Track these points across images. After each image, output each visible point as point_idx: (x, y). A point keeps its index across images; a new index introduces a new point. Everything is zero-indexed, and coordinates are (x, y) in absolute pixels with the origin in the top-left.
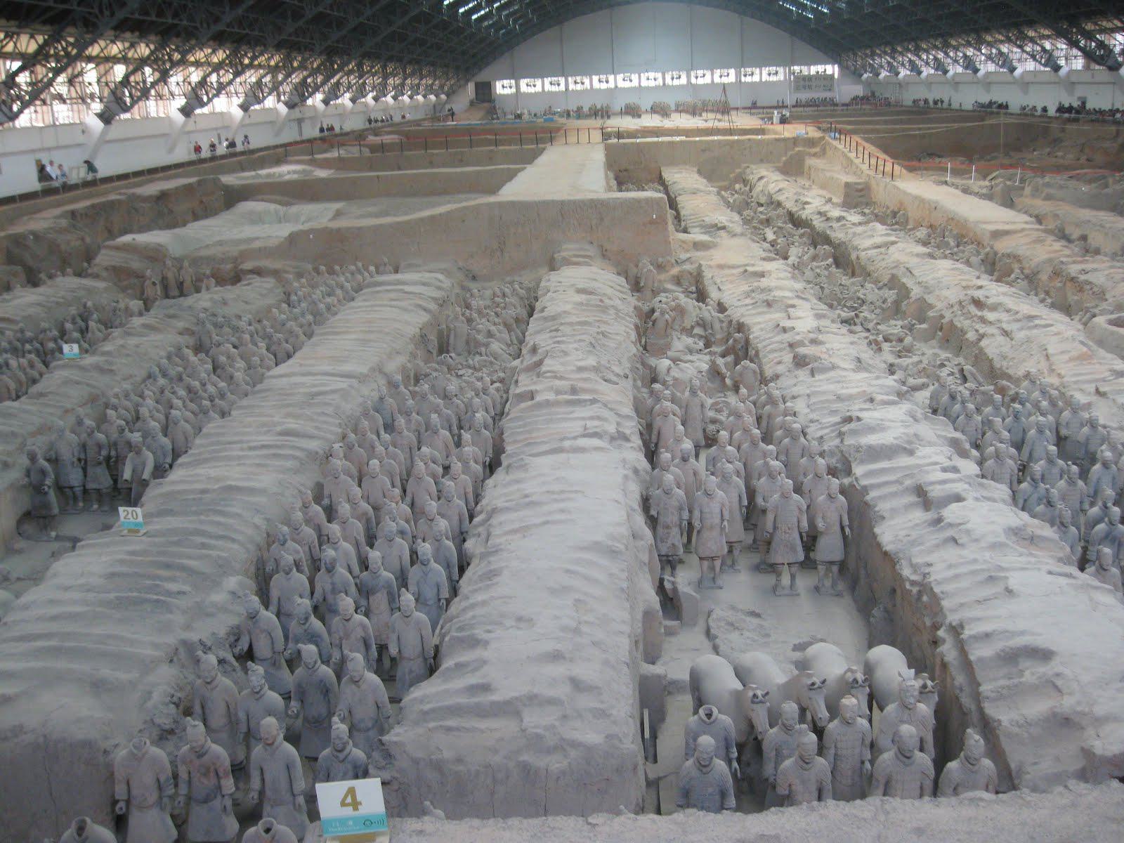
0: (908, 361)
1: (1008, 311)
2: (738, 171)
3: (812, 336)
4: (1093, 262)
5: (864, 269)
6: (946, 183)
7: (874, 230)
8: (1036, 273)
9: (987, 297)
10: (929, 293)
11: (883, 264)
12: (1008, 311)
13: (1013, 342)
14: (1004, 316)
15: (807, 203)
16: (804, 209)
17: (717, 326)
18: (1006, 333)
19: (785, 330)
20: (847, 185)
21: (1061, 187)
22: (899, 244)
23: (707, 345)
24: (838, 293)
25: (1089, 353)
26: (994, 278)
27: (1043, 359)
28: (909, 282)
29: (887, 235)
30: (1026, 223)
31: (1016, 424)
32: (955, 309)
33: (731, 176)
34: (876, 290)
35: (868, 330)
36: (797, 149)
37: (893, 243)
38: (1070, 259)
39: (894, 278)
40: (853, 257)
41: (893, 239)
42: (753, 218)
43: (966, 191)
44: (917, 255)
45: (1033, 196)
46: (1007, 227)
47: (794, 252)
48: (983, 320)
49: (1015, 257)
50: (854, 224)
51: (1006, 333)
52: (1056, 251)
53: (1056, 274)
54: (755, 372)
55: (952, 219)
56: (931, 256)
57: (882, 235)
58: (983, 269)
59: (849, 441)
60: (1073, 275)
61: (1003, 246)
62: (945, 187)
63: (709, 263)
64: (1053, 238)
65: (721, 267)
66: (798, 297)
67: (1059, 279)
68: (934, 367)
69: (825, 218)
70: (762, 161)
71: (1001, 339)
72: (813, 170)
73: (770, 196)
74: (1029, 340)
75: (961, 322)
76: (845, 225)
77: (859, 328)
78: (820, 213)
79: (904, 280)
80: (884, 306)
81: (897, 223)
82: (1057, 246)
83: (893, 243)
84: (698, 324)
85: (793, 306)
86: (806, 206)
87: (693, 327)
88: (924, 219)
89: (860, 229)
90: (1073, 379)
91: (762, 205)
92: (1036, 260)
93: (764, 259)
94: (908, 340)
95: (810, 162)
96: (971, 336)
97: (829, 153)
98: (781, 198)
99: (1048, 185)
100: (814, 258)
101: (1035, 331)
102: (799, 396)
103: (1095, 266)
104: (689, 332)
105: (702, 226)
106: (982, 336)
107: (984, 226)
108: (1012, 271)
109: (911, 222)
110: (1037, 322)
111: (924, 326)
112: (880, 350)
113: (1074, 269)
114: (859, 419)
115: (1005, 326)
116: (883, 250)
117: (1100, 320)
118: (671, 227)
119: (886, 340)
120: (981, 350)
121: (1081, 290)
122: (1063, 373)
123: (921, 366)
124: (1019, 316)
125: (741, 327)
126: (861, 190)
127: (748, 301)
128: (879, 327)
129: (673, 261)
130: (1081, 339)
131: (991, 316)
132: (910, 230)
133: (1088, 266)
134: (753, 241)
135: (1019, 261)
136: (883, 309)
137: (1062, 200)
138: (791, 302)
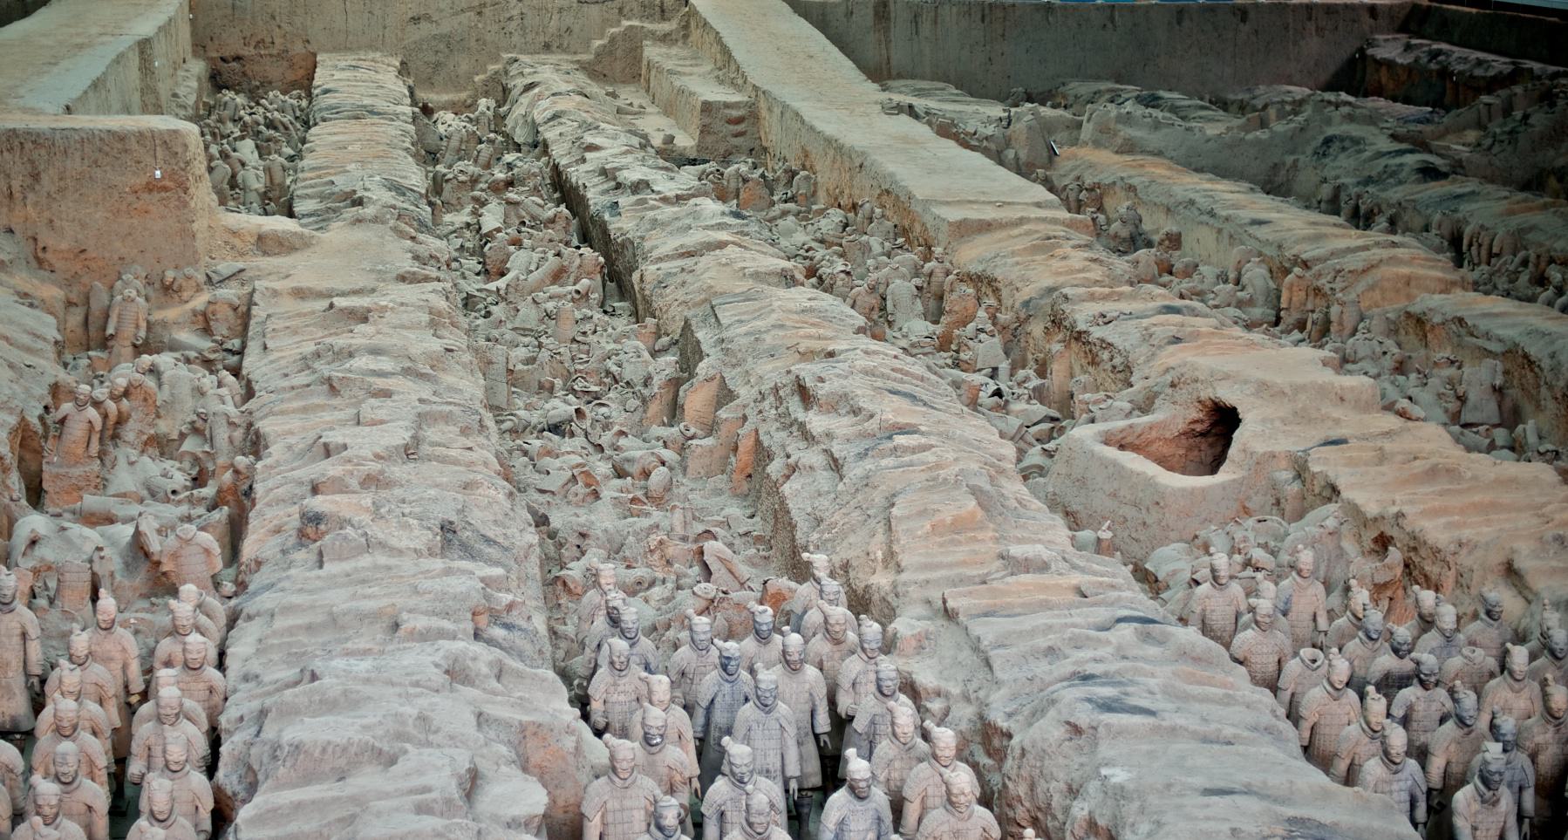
0: (645, 522)
1: (855, 412)
2: (492, 68)
3: (374, 467)
4: (1132, 297)
5: (648, 302)
6: (911, 111)
7: (696, 215)
8: (1022, 322)
9: (821, 380)
10: (734, 366)
11: (680, 295)
12: (855, 412)
13: (841, 487)
14: (841, 425)
15: (592, 148)
16: (584, 160)
17: (222, 434)
18: (836, 465)
19: (328, 452)
20: (707, 107)
21: (1157, 125)
22: (730, 248)
23: (198, 481)
24: (567, 357)
25: (980, 514)
26: (939, 329)
27: (881, 529)
28: (703, 335)
29: (720, 226)
30: (1038, 205)
31: (727, 685)
32: (766, 404)
33: (477, 79)
34: (646, 355)
35: (600, 448)
36: (626, 23)
37: (722, 245)
38: (1082, 290)
39: (687, 326)
40: (636, 276)
41: (723, 236)
42: (474, 181)
43: (946, 130)
44: (757, 276)
45: (1097, 144)
46: (989, 214)
47: (518, 260)
48: (807, 436)
49: (991, 281)
50: (665, 200)
51: (836, 465)
52: (1072, 271)
53: (1057, 322)
54: (207, 551)
55: (888, 192)
56: (788, 280)
57: (706, 228)
58: (919, 306)
59: (269, 733)
60: (1081, 326)
61: (971, 255)
62: (904, 118)
63: (277, 285)
64: (1085, 238)
65: (300, 294)
66: (406, 372)
67: (1060, 336)
68: (684, 539)
69: (613, 184)
70: (547, 47)
71: (824, 478)
72: (653, 73)
73: (535, 128)
74: (867, 482)
75: (774, 437)
76: (644, 201)
77: (579, 441)
78: (604, 172)
79: (700, 335)
80: (646, 392)
81: (792, 199)
82: (1078, 258)
83: (722, 245)
84: (196, 431)
85: (387, 394)
86: (588, 155)
87: (183, 436)
88: (842, 192)
89: (669, 211)
90: (922, 577)
91: (518, 148)
92: (1026, 293)
93: (402, 278)
94: (659, 475)
95: (652, 52)
96: (775, 468)
97: (695, 34)
98: (549, 134)
99: (1127, 119)
100: (558, 276)
101: (888, 462)
102: (258, 614)
103: (1125, 306)
104: (161, 446)
105: (322, 197)
106: (793, 469)
107: (936, 210)
108: (972, 318)
109: (821, 194)
110: (900, 440)
111: (709, 442)
112: (596, 495)
113: (1082, 315)
114: (314, 677)
115: (836, 449)
116: (688, 262)
117: (1082, 434)
118: (203, 194)
119: (620, 473)
120: (782, 502)
121: (1094, 362)
122: (905, 560)
123: (654, 540)
124: (871, 425)
125: (255, 444)
126: (739, 120)
127: (302, 379)
128: (622, 442)
129: (201, 278)
130: (983, 483)
131: (817, 422)
132: (821, 212)
133: (1110, 308)
134: (401, 234)
135: (996, 291)
136: (644, 401)
137: (1159, 154)
138: (380, 383)
